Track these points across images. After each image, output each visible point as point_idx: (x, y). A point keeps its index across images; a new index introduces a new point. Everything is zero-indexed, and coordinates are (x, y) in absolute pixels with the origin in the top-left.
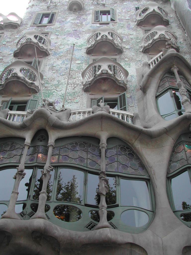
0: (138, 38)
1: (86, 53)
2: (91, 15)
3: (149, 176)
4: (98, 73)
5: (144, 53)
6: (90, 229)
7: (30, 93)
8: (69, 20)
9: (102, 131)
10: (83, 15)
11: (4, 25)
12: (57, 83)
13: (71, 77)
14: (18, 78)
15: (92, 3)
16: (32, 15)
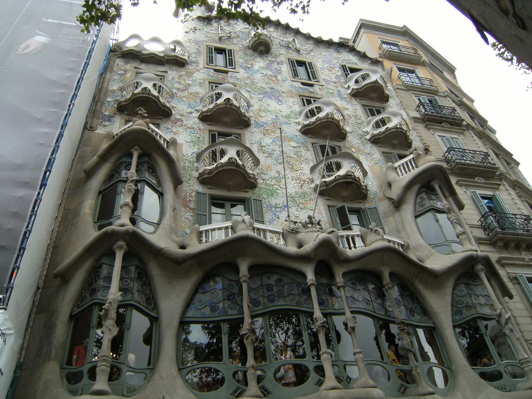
0: (357, 116)
1: (300, 131)
2: (285, 65)
3: (434, 324)
4: (342, 172)
6: (403, 393)
7: (246, 187)
8: (256, 67)
9: (383, 265)
10: (272, 62)
11: (166, 58)
12: (277, 175)
13: (292, 168)
14: (238, 165)
15: (279, 43)
16: (199, 47)
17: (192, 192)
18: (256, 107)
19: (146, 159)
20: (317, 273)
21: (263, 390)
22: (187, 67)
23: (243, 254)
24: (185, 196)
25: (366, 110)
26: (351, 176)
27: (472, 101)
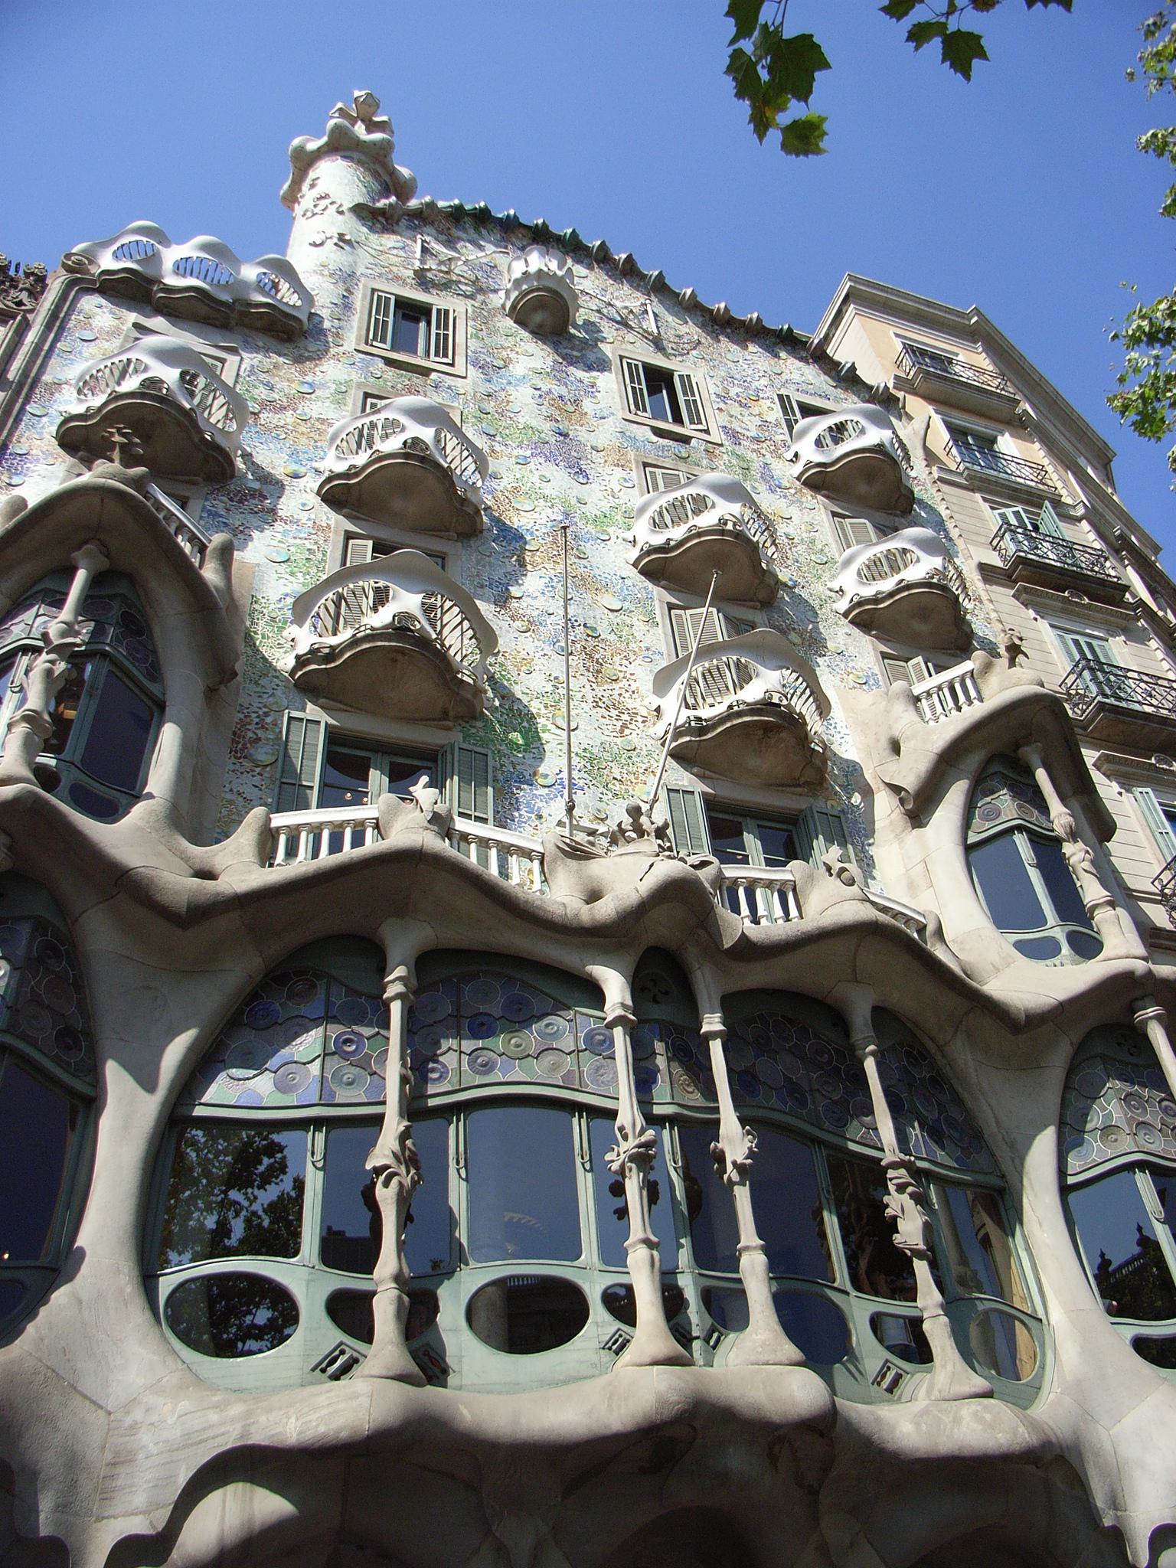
0: (813, 542)
1: (635, 565)
5: (851, 622)
12: (549, 688)
16: (347, 290)
17: (266, 714)
18: (504, 483)
19: (123, 588)
20: (638, 987)
21: (426, 1359)
22: (302, 343)
23: (402, 909)
24: (243, 724)
25: (843, 529)
26: (779, 706)
27: (1157, 549)
